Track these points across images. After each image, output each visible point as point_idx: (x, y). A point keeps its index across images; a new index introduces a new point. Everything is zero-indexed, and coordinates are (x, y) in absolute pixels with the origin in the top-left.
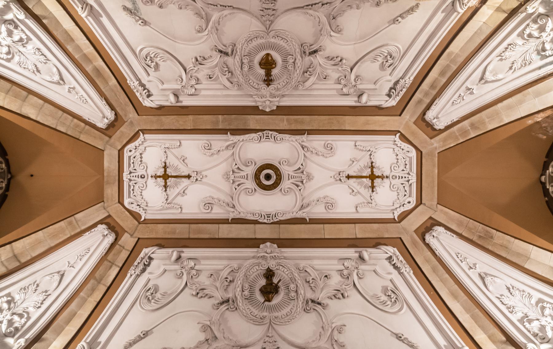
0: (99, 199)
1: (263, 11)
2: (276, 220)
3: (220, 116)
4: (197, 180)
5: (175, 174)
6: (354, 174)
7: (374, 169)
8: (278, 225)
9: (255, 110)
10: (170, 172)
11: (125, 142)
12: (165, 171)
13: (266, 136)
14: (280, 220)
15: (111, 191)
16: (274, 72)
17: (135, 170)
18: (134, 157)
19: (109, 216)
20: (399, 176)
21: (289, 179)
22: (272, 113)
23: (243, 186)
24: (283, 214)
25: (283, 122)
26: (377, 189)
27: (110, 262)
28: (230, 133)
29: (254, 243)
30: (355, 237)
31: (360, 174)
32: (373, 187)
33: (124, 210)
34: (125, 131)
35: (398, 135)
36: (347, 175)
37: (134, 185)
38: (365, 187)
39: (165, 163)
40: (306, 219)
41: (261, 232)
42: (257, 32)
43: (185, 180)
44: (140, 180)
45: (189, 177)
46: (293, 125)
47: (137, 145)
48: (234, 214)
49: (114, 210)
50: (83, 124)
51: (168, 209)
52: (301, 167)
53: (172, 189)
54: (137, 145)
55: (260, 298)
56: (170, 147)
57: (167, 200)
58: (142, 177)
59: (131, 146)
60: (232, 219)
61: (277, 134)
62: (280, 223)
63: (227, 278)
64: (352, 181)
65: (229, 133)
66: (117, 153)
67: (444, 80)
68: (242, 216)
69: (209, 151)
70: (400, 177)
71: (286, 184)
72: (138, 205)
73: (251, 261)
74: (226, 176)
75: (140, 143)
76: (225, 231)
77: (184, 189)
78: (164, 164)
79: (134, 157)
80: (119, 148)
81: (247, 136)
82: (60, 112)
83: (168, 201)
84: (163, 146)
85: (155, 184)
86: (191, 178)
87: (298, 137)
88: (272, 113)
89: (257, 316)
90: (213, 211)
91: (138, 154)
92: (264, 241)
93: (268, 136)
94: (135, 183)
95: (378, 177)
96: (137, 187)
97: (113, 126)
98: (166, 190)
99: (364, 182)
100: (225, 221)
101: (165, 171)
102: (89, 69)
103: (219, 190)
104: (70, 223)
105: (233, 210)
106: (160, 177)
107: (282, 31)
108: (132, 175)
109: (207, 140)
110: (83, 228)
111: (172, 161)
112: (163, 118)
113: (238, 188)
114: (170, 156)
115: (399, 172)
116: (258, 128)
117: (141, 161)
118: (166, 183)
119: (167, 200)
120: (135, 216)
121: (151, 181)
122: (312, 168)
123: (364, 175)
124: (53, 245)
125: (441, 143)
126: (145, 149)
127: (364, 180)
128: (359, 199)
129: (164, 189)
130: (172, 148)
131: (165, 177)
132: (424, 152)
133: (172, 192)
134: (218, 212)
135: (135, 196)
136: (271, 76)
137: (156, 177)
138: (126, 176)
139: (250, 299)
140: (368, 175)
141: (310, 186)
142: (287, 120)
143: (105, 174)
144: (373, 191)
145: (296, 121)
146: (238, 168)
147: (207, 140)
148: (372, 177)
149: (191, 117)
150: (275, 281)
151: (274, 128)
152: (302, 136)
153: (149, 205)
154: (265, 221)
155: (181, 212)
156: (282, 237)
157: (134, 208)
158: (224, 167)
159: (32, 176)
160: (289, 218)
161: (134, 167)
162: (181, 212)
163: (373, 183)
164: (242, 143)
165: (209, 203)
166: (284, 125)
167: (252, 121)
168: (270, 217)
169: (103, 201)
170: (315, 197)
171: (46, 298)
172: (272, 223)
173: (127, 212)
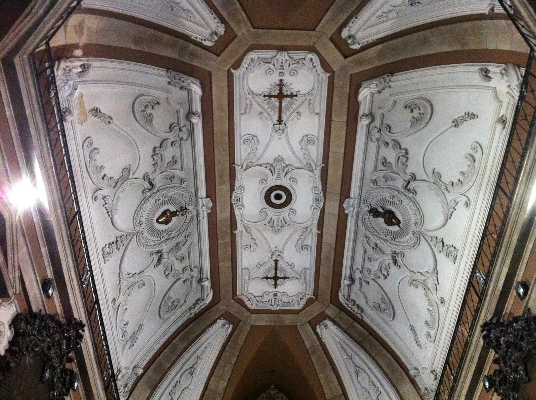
0: (294, 329)
1: (119, 248)
2: (322, 194)
3: (219, 242)
4: (279, 255)
5: (274, 271)
6: (277, 114)
7: (271, 94)
8: (327, 194)
9: (212, 217)
10: (272, 282)
11: (245, 310)
12: (271, 278)
13: (237, 201)
14: (323, 190)
15: (288, 320)
16: (173, 209)
17: (269, 301)
18: (258, 301)
19: (309, 322)
20: (280, 69)
21: (282, 180)
22: (214, 202)
23: (287, 219)
24: (317, 187)
25: (223, 188)
26: (294, 91)
27: (349, 328)
28: (234, 231)
29: (342, 218)
30: (346, 124)
31: (277, 109)
32: (292, 96)
33: (304, 311)
34: (234, 309)
35: (232, 71)
36: (278, 123)
37: (282, 302)
38: (293, 103)
39: (263, 278)
40: (323, 167)
41: (333, 208)
42: (138, 240)
43: (279, 263)
44: (278, 298)
45: (276, 261)
46: (225, 179)
47: (247, 299)
48: (314, 228)
49: (303, 318)
50: (230, 343)
51: (305, 279)
52: (268, 168)
53: (288, 274)
54: (247, 299)
55: (395, 228)
56: (249, 276)
57: (297, 278)
58: (275, 295)
59: (248, 304)
60: (318, 229)
61: (234, 192)
62: (324, 190)
63: (373, 248)
64: (284, 118)
65: (235, 232)
66: (254, 316)
67: (167, 36)
68: (315, 222)
69: (252, 247)
70: (282, 68)
71: (285, 182)
72: (301, 300)
73: (360, 222)
74: (277, 231)
75: (245, 297)
76: (329, 236)
77: (287, 265)
78: (264, 279)
79: (258, 301)
80: (249, 313)
81: (237, 217)
82: (221, 362)
83: (298, 277)
84: (248, 281)
85: (282, 286)
86: (278, 259)
87: (238, 174)
88: (214, 202)
89: (412, 239)
90: (310, 244)
91: (255, 299)
92: (341, 208)
93: (237, 199)
94: (281, 301)
95: (281, 90)
96: (284, 300)
97: (229, 317)
98: (288, 278)
99: (285, 105)
100: (320, 237)
101: (271, 278)
102: (182, 346)
103: (290, 237)
104: (314, 352)
105: (309, 229)
106: (276, 283)
107: (134, 221)
108: (273, 304)
109: (242, 248)
110: (318, 343)
111: (261, 272)
112: (222, 284)
113: (288, 223)
114: (257, 275)
115: (276, 68)
116: (229, 210)
117: (261, 296)
118: (281, 278)
119: (297, 278)
120: (309, 302)
121: (280, 289)
122: (269, 156)
123: (278, 104)
124: (330, 368)
125: (241, 25)
126: (251, 294)
127: (284, 104)
128: (304, 109)
129: (288, 279)
130: (250, 274)
131: (276, 278)
132: (252, 42)
133: (289, 273)
134: (311, 241)
135: (292, 301)
136: (177, 211)
137: (275, 286)
138: (275, 308)
139: (395, 237)
140: (278, 100)
141: (289, 158)
142: (221, 185)
143: (273, 324)
144: (296, 96)
145: (221, 177)
146: (269, 223)
147: (242, 248)
148: (281, 96)
149: (221, 264)
150: (381, 210)
151: (229, 196)
152: (236, 169)
153: (301, 291)
154: (322, 203)
155: (310, 269)
156: (339, 192)
157: (302, 303)
158: (268, 234)
159: (273, 371)
160: (320, 182)
161: (266, 302)
162: (310, 269)
163: (287, 96)
164: (244, 221)
165: (302, 248)
166: (226, 187)
167: (223, 215)
168: (318, 199)
169: (296, 326)
170: (300, 154)
171: (372, 382)
172: (325, 197)
173: (307, 309)
